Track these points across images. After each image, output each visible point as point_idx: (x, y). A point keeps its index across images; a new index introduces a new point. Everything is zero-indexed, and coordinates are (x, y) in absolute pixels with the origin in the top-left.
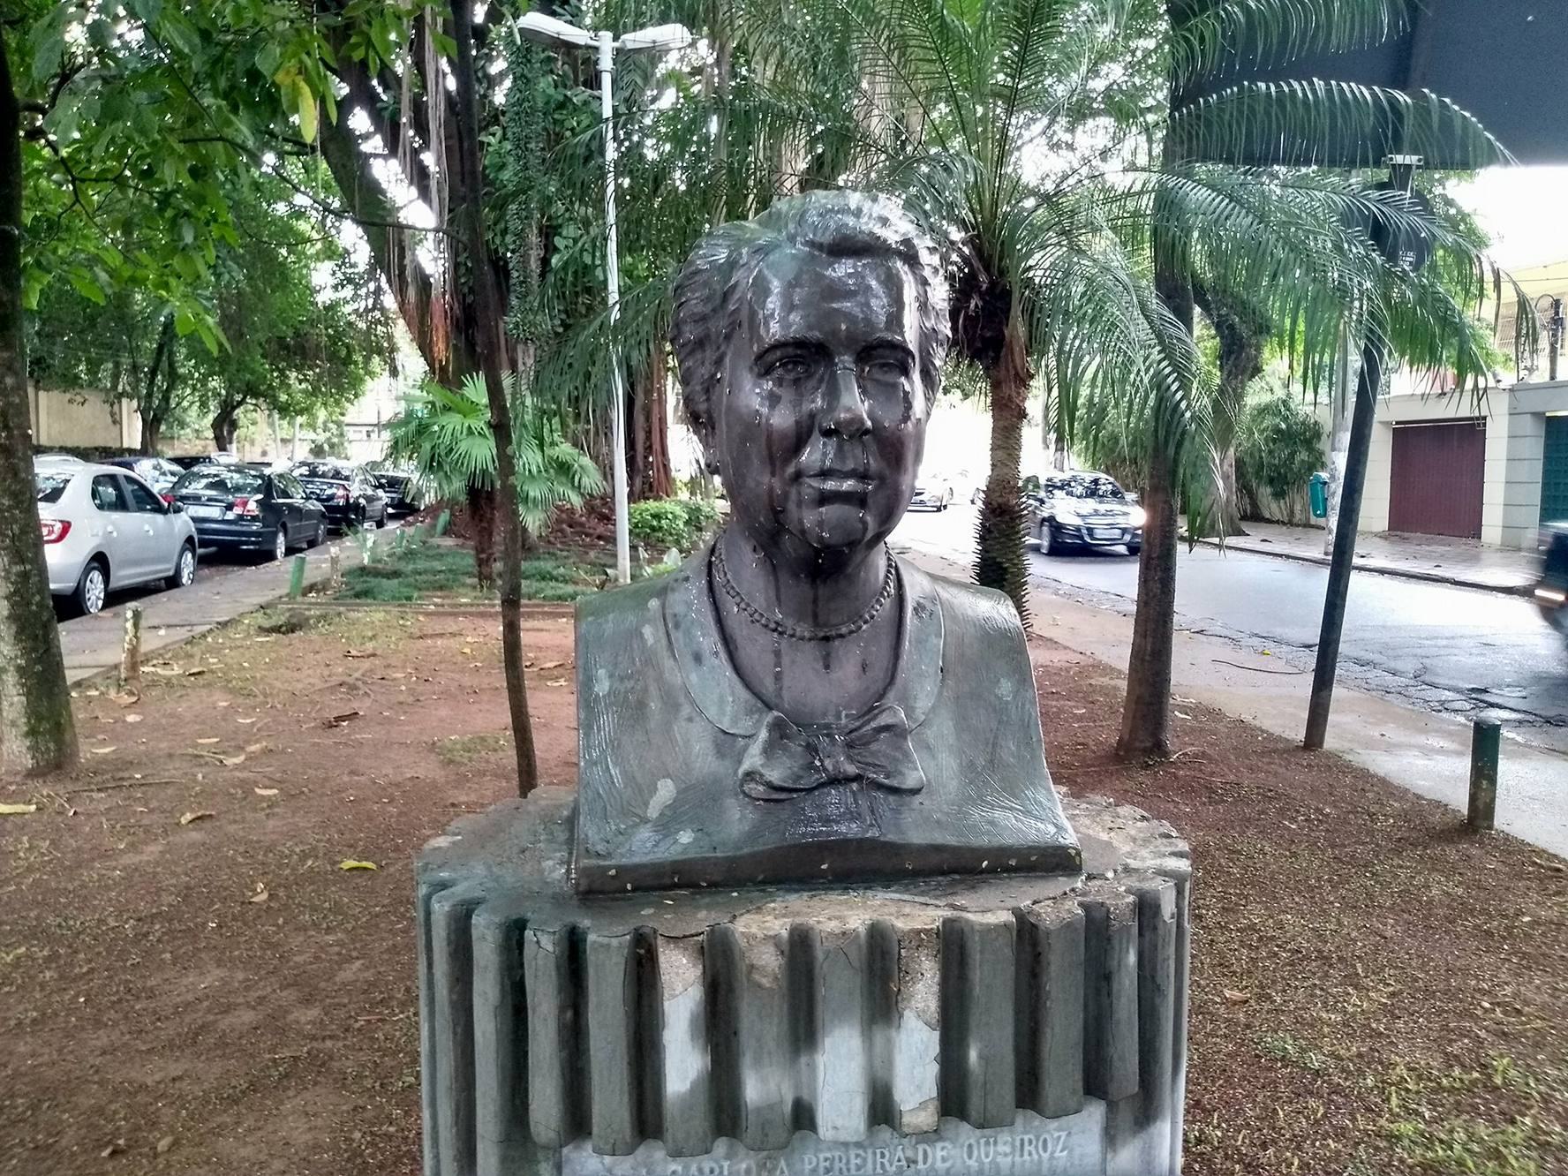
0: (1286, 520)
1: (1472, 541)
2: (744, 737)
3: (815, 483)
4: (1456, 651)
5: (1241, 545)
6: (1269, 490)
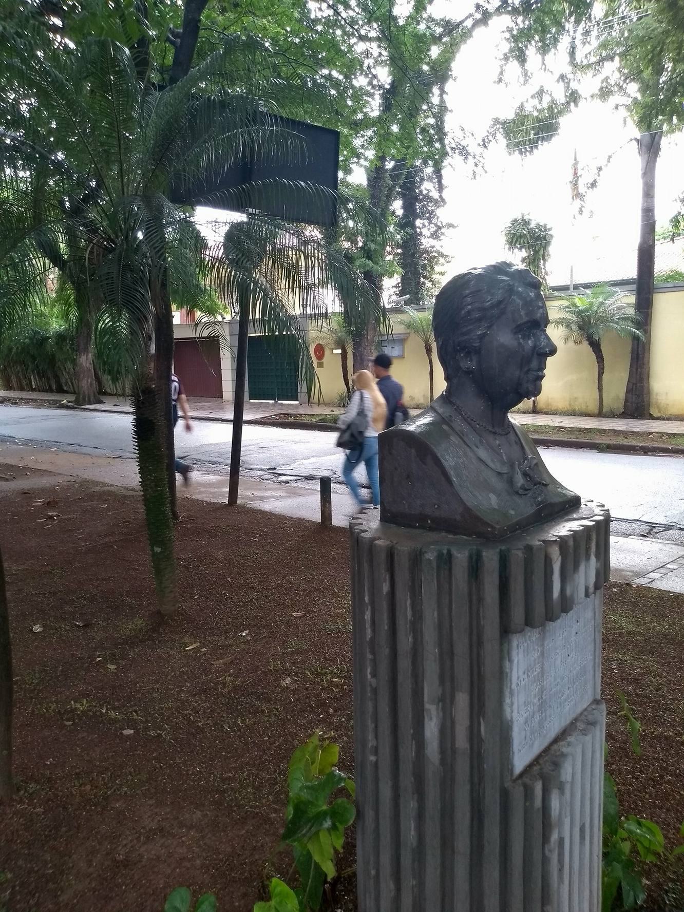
0: (120, 392)
1: (219, 399)
2: (506, 473)
3: (535, 373)
4: (252, 452)
5: (104, 409)
6: (109, 377)
